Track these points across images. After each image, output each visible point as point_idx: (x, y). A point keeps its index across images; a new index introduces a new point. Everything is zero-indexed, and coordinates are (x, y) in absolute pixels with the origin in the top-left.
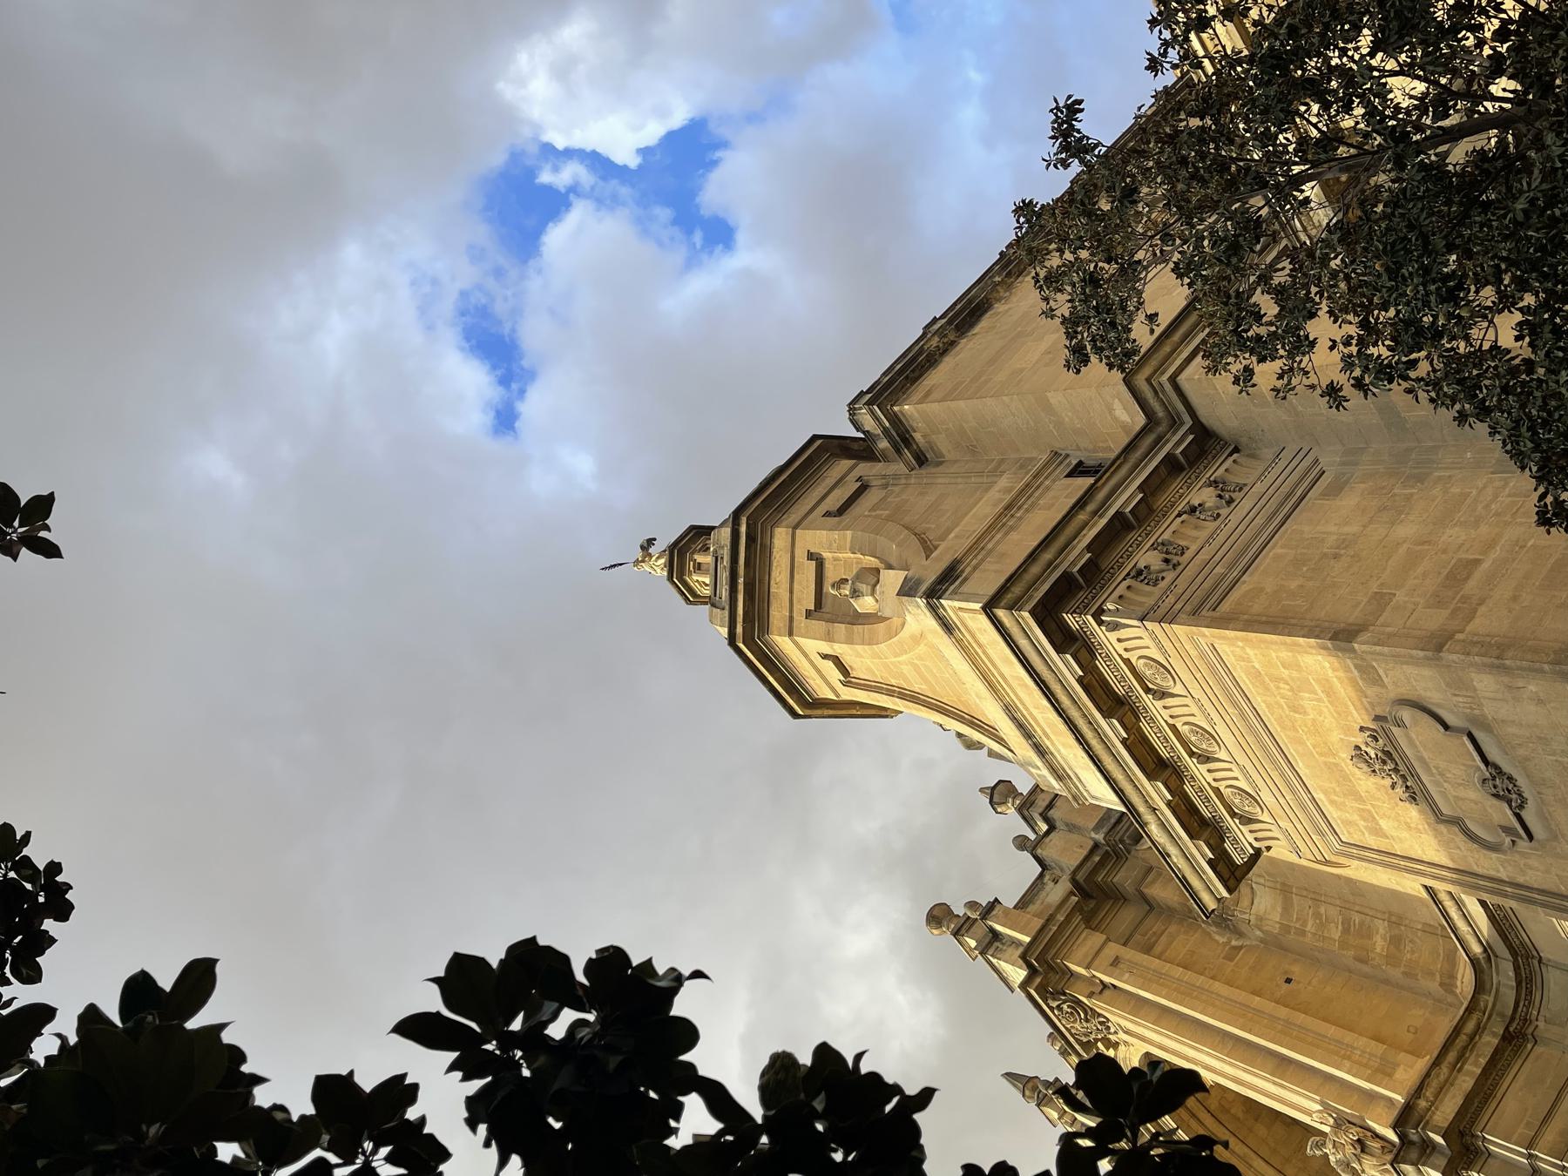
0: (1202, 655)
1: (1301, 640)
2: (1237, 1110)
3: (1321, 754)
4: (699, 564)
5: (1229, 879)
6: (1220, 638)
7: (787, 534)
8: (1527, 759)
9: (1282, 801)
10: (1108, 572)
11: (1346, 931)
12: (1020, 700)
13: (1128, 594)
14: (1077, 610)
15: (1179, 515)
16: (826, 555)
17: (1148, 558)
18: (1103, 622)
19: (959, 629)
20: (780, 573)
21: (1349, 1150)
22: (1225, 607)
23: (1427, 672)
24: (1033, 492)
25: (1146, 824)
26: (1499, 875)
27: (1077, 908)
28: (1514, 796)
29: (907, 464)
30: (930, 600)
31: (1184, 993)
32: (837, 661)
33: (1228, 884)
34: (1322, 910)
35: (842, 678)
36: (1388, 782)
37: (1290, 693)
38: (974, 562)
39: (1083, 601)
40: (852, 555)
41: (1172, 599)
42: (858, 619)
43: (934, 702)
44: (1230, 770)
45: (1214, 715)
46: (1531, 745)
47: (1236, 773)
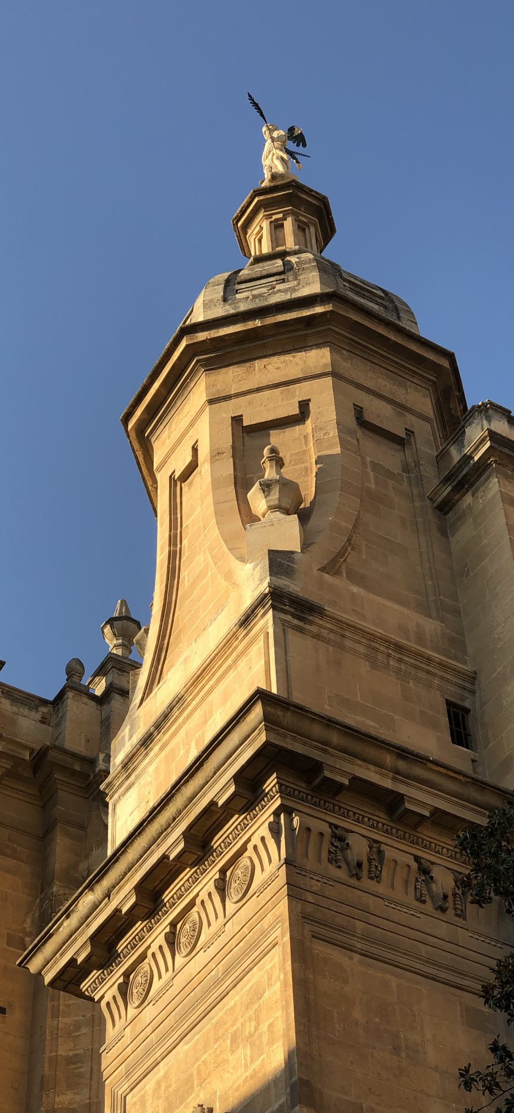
0: (265, 933)
3: (199, 1071)
4: (282, 226)
7: (325, 365)
9: (149, 1030)
10: (335, 805)
11: (70, 1061)
12: (191, 714)
13: (314, 837)
14: (283, 787)
15: (417, 859)
16: (309, 422)
18: (279, 816)
19: (246, 635)
20: (278, 368)
22: (320, 948)
24: (422, 669)
25: (92, 890)
27: (18, 761)
29: (435, 493)
30: (269, 597)
33: (58, 981)
34: (84, 1030)
35: (177, 475)
38: (325, 633)
39: (295, 790)
40: (314, 460)
41: (316, 886)
42: (242, 484)
43: (174, 599)
44: (167, 970)
47: (166, 976)
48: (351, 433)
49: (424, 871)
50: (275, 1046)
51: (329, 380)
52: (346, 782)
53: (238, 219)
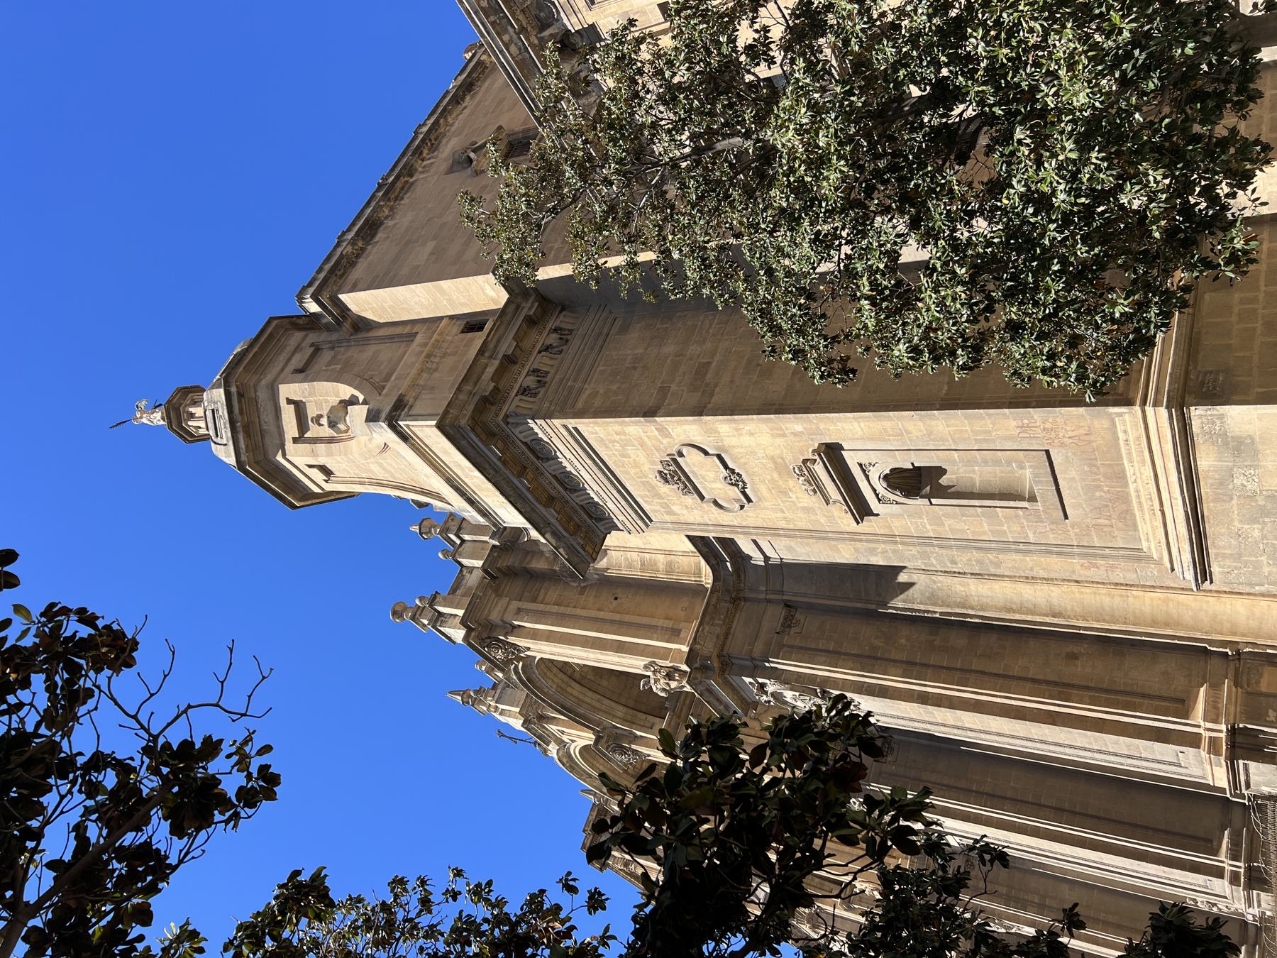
1: (627, 419)
2: (590, 676)
3: (639, 477)
21: (662, 681)
22: (580, 405)
23: (694, 427)
31: (562, 619)
36: (676, 486)
48: (307, 376)
49: (547, 348)
53: (185, 440)
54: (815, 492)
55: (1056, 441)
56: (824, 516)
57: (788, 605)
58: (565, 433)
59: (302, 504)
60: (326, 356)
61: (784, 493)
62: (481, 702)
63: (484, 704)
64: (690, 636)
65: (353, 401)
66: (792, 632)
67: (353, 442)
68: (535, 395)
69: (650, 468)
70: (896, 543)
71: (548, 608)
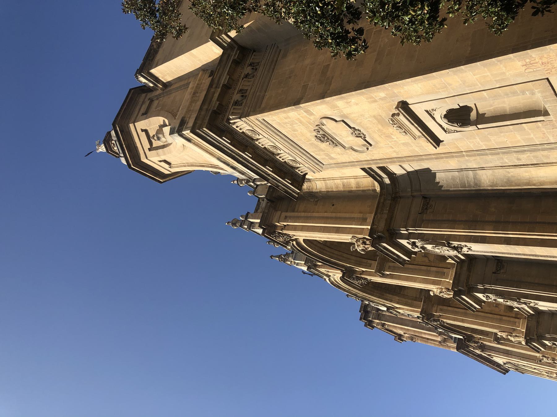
3: (308, 141)
5: (298, 187)
6: (265, 116)
8: (361, 123)
17: (236, 97)
21: (361, 246)
22: (263, 105)
26: (367, 159)
28: (362, 135)
32: (165, 161)
33: (299, 188)
34: (336, 182)
36: (328, 143)
37: (291, 126)
41: (247, 108)
45: (274, 141)
46: (360, 118)
49: (246, 76)
50: (290, 116)
51: (136, 124)
52: (218, 102)
53: (116, 156)
54: (406, 133)
55: (553, 70)
56: (417, 146)
57: (424, 197)
58: (259, 123)
59: (164, 180)
60: (156, 103)
61: (388, 136)
62: (287, 260)
63: (289, 261)
64: (370, 220)
65: (165, 125)
66: (428, 212)
67: (171, 146)
68: (241, 105)
69: (311, 135)
70: (463, 156)
71: (299, 214)
